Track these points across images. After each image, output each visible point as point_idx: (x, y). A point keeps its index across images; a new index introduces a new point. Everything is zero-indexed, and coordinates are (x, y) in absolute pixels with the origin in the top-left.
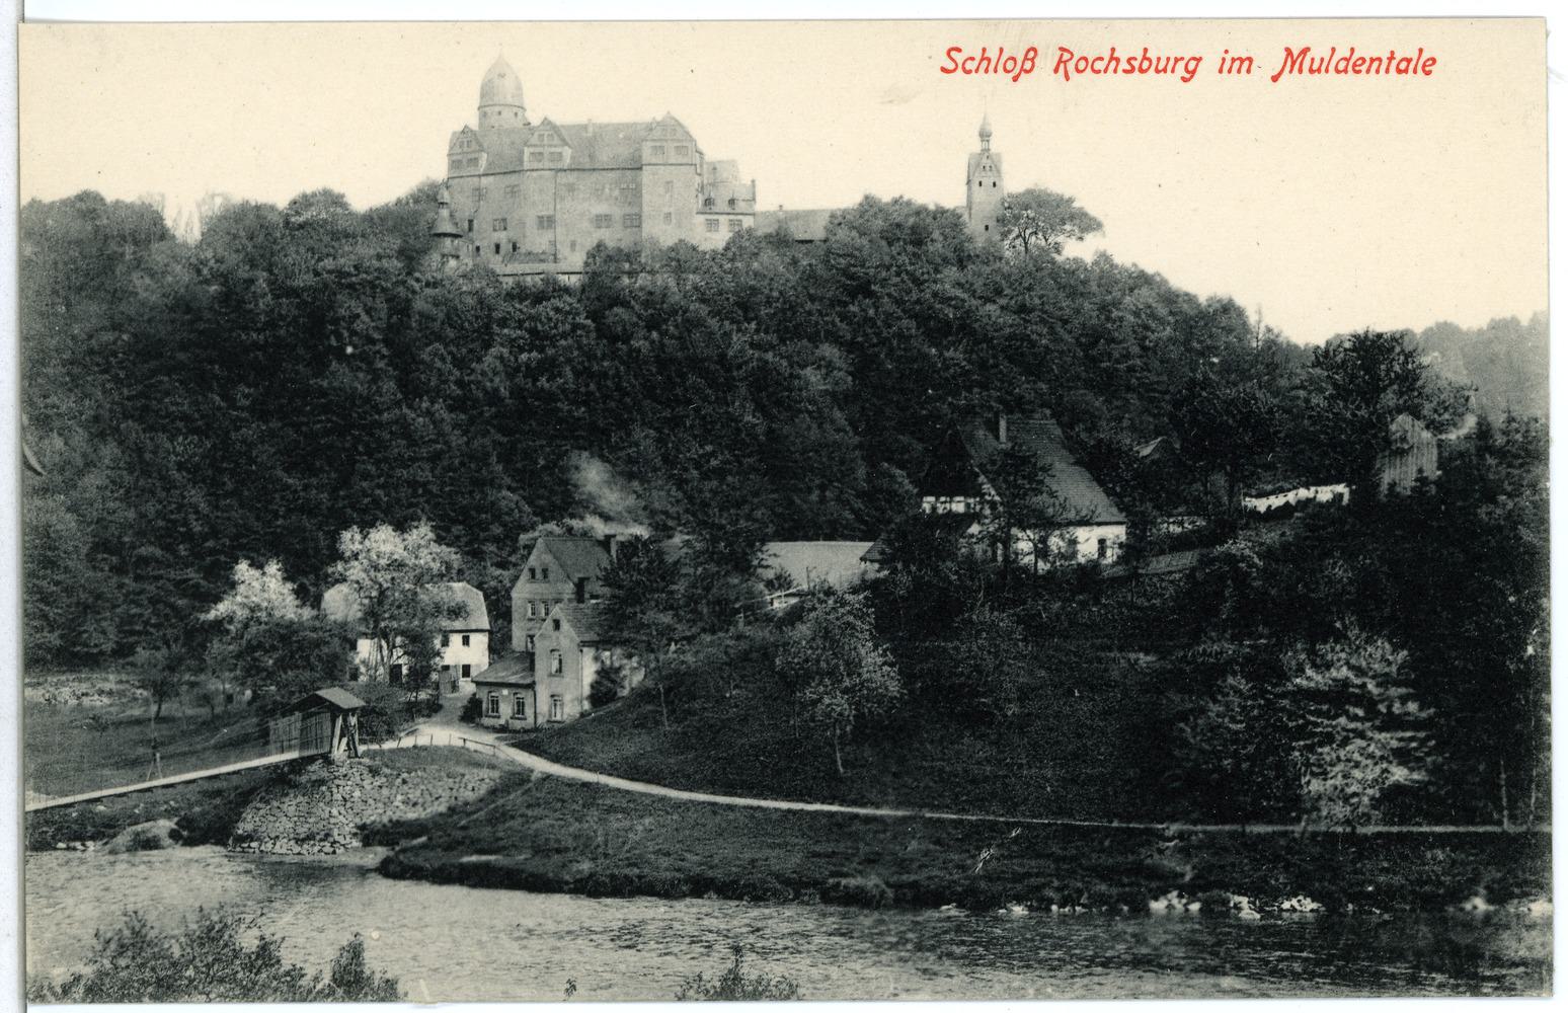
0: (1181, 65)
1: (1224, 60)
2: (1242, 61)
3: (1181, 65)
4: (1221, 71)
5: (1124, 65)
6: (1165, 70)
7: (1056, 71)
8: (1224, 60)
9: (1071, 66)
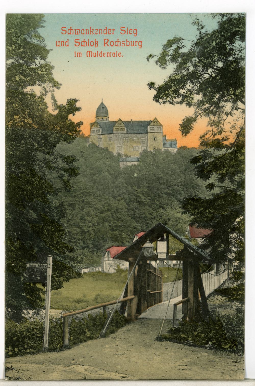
0: (137, 43)
1: (75, 53)
2: (79, 53)
3: (137, 43)
4: (75, 56)
5: (121, 44)
6: (133, 46)
7: (105, 46)
8: (75, 53)
9: (109, 43)
